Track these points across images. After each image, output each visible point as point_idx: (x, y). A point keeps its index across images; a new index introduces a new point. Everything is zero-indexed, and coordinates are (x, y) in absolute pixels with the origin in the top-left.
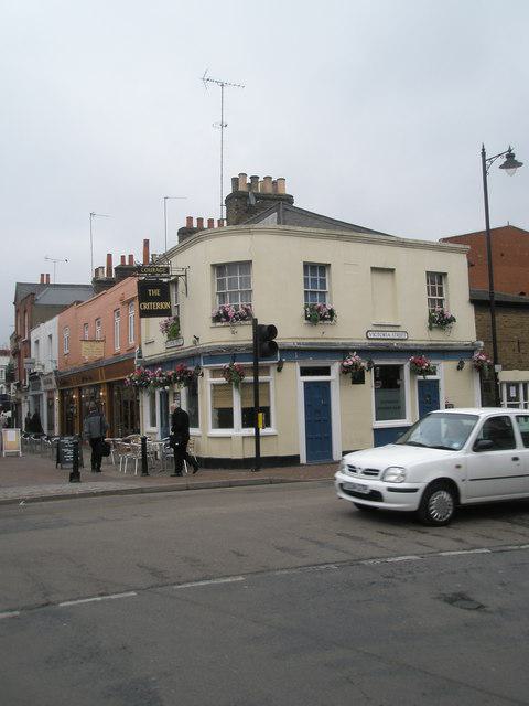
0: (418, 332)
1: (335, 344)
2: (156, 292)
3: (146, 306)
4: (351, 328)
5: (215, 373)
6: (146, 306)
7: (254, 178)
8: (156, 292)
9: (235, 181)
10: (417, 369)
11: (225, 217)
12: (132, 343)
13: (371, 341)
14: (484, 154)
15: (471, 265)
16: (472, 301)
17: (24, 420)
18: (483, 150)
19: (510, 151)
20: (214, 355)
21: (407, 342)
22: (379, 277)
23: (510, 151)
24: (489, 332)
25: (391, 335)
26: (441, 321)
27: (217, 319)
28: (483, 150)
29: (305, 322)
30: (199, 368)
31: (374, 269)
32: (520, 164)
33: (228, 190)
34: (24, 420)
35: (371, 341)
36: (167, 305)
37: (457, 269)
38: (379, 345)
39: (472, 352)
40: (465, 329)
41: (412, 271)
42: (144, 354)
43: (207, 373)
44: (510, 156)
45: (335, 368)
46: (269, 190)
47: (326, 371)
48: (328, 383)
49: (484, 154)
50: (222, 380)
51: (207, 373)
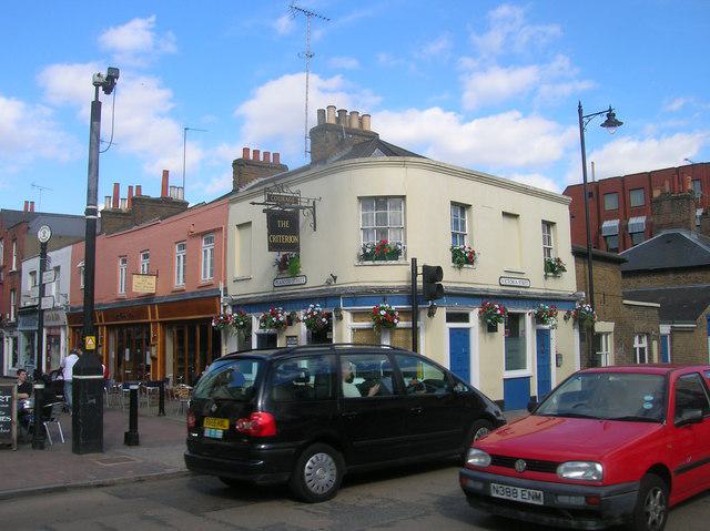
0: (538, 283)
1: (475, 290)
2: (285, 224)
3: (275, 239)
4: (484, 276)
5: (356, 315)
6: (275, 239)
7: (342, 112)
8: (285, 224)
9: (321, 113)
10: (539, 319)
11: (309, 150)
12: (206, 277)
13: (504, 288)
14: (580, 111)
15: (572, 217)
16: (573, 253)
17: (671, 386)
18: (580, 107)
19: (610, 110)
20: (355, 296)
21: (528, 290)
22: (507, 221)
23: (610, 110)
24: (587, 282)
25: (517, 282)
26: (553, 268)
27: (366, 257)
28: (580, 107)
29: (452, 264)
30: (338, 310)
31: (505, 214)
32: (621, 123)
33: (314, 122)
34: (671, 386)
35: (504, 288)
36: (296, 239)
37: (561, 215)
38: (509, 292)
39: (574, 301)
40: (567, 284)
41: (533, 212)
42: (230, 292)
43: (347, 316)
44: (611, 115)
45: (474, 315)
46: (355, 124)
47: (464, 317)
48: (468, 330)
49: (580, 111)
50: (365, 324)
51: (347, 316)
